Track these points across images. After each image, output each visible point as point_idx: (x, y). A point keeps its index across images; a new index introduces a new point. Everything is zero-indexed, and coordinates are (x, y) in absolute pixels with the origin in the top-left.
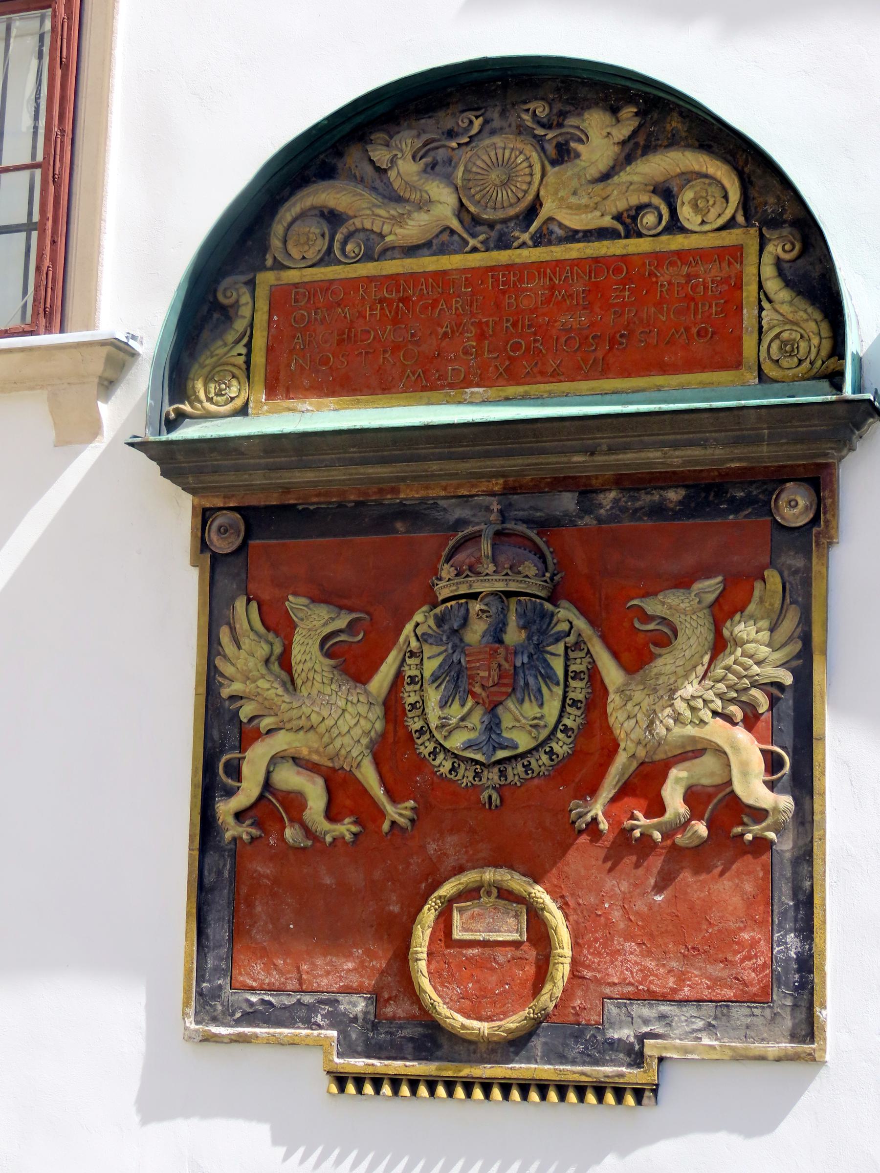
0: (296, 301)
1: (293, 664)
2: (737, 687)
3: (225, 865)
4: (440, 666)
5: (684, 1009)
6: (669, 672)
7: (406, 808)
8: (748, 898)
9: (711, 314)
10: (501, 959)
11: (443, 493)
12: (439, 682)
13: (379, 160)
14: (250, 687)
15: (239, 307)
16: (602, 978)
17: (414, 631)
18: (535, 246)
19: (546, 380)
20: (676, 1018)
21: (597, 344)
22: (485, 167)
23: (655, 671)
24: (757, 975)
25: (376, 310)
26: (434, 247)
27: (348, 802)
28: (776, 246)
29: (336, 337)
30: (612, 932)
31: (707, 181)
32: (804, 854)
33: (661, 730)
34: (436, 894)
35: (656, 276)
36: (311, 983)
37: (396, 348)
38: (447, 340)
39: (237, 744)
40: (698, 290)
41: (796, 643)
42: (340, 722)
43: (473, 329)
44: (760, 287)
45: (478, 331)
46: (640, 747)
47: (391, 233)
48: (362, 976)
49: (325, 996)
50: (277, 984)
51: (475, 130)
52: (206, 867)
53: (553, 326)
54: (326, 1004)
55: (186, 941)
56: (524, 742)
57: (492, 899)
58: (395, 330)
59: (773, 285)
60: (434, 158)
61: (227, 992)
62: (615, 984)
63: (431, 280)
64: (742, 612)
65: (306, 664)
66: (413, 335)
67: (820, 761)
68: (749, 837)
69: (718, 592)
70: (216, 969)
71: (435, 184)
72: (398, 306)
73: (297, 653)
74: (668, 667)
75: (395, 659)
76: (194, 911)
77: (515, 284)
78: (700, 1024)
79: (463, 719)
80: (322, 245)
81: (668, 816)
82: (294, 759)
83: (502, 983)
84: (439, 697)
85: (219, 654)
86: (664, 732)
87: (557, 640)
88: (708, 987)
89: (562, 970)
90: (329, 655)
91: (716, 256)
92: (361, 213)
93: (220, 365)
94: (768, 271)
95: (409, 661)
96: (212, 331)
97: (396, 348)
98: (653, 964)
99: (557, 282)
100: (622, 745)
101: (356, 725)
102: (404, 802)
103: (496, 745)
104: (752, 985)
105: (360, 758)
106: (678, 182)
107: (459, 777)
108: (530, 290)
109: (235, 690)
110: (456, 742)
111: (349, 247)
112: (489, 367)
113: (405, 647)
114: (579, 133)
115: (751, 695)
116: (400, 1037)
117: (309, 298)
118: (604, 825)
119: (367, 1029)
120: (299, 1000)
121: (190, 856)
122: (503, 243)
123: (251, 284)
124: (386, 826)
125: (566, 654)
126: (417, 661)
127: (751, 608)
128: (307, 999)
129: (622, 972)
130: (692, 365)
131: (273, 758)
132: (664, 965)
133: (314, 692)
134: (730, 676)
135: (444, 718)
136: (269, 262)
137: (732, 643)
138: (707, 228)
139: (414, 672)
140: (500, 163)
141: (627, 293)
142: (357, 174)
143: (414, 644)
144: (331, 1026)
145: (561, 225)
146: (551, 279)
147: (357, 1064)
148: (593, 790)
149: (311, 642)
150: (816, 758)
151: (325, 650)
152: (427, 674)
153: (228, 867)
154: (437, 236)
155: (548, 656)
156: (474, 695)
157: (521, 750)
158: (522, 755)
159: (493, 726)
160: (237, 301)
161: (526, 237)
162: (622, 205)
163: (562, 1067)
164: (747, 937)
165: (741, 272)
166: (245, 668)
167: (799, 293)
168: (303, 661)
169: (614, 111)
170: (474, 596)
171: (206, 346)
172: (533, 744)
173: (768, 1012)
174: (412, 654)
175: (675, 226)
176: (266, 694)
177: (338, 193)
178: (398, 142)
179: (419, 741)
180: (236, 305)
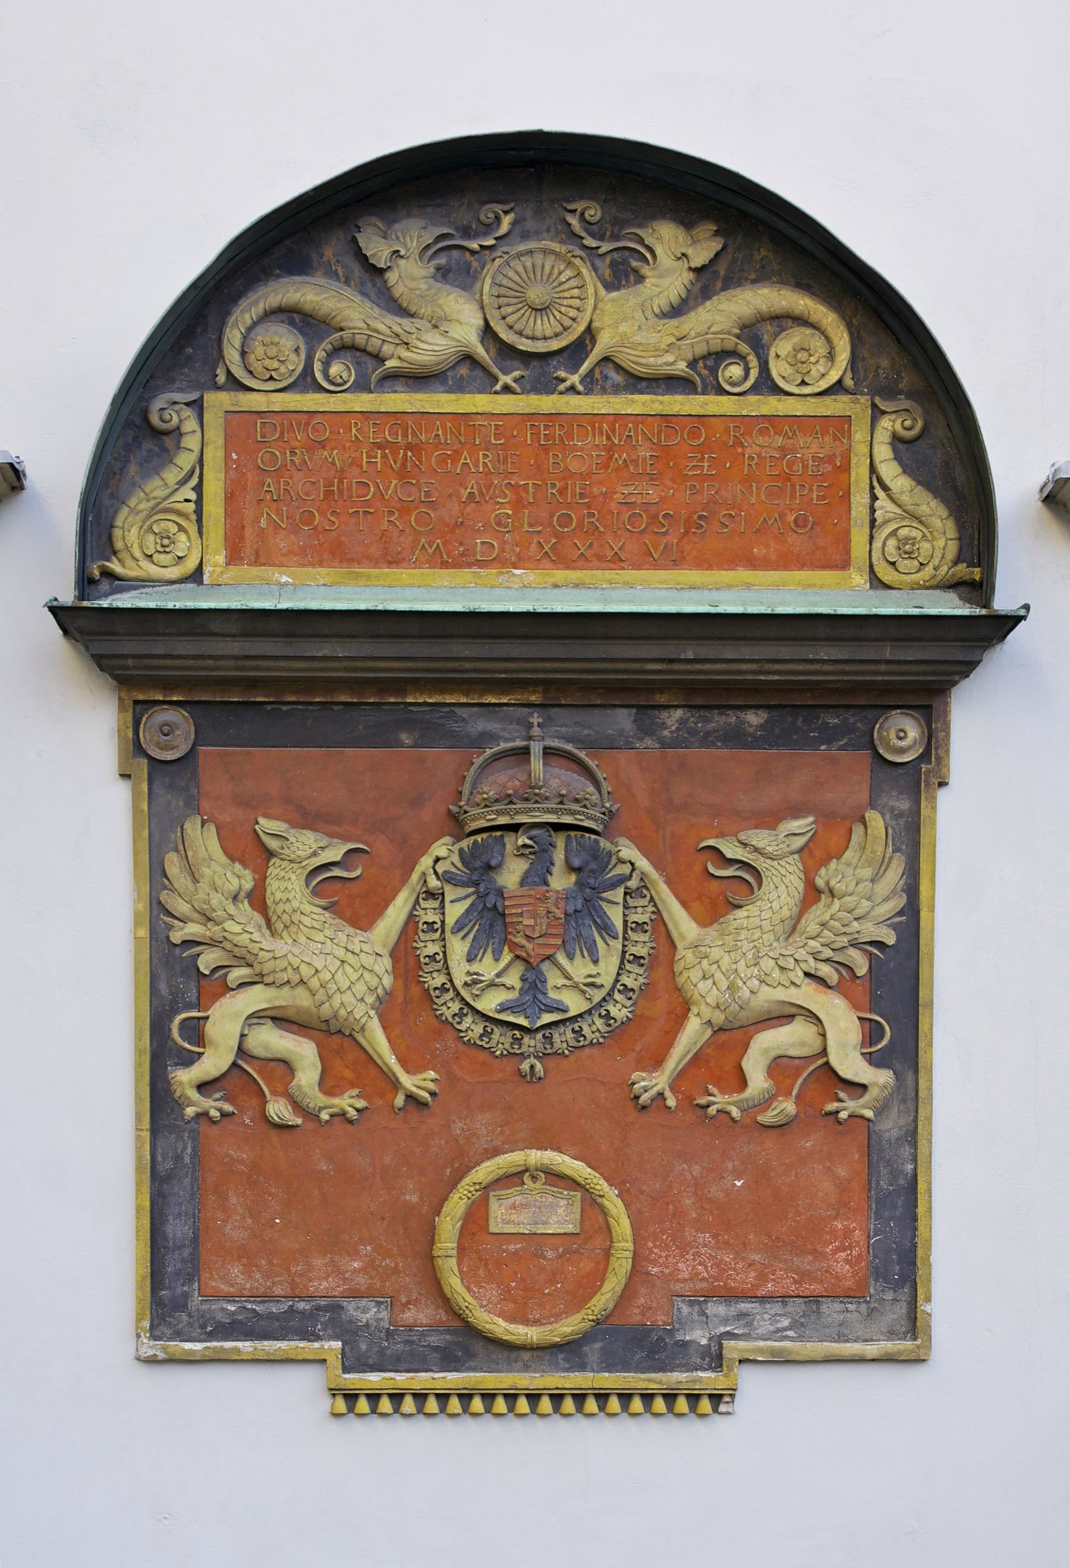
0: (263, 436)
1: (269, 902)
2: (832, 947)
3: (185, 1148)
4: (467, 911)
5: (768, 1306)
6: (753, 926)
7: (425, 1080)
8: (841, 1183)
9: (812, 499)
10: (550, 1254)
11: (464, 700)
12: (466, 930)
13: (372, 255)
14: (215, 930)
15: (181, 435)
16: (671, 1274)
17: (434, 868)
18: (586, 394)
19: (605, 565)
20: (758, 1317)
21: (670, 525)
22: (518, 279)
23: (735, 924)
24: (852, 1268)
25: (376, 457)
26: (450, 383)
27: (348, 1074)
28: (894, 421)
29: (322, 488)
30: (681, 1222)
31: (808, 331)
32: (906, 1135)
33: (745, 993)
34: (467, 1180)
35: (743, 446)
36: (306, 1288)
37: (405, 509)
38: (472, 504)
39: (194, 1000)
40: (795, 468)
41: (901, 896)
42: (339, 976)
43: (507, 492)
44: (873, 469)
45: (514, 497)
46: (717, 1012)
47: (392, 357)
48: (372, 1278)
49: (323, 1302)
50: (262, 1290)
51: (504, 228)
52: (160, 1150)
53: (612, 499)
54: (327, 1311)
55: (138, 1240)
56: (575, 1004)
57: (538, 1185)
58: (402, 486)
59: (889, 470)
60: (448, 263)
61: (196, 1300)
62: (685, 1280)
63: (449, 425)
64: (838, 859)
65: (288, 904)
66: (428, 494)
67: (926, 1030)
68: (843, 1115)
69: (810, 835)
70: (178, 1273)
71: (452, 296)
72: (405, 455)
73: (275, 888)
74: (751, 920)
75: (406, 901)
76: (147, 1204)
77: (562, 440)
78: (786, 1322)
79: (498, 975)
80: (296, 364)
81: (749, 1093)
82: (274, 1019)
83: (552, 1281)
84: (466, 949)
85: (165, 888)
86: (747, 993)
87: (613, 885)
88: (795, 1282)
89: (621, 1265)
90: (315, 893)
91: (817, 427)
92: (351, 325)
93: (154, 514)
94: (883, 452)
95: (424, 904)
96: (141, 464)
97: (405, 509)
98: (731, 1257)
99: (616, 442)
100: (695, 1010)
101: (358, 979)
102: (421, 1073)
103: (543, 1008)
104: (845, 1278)
105: (364, 1020)
106: (769, 328)
107: (493, 1043)
108: (581, 449)
109: (191, 934)
110: (489, 1003)
111: (335, 369)
112: (530, 544)
113: (419, 887)
114: (643, 250)
115: (848, 956)
116: (422, 1346)
117: (282, 433)
118: (671, 1102)
119: (381, 1338)
120: (291, 1307)
121: (138, 1138)
122: (546, 385)
123: (197, 406)
124: (400, 1100)
125: (625, 900)
126: (436, 904)
127: (848, 854)
128: (302, 1305)
129: (694, 1267)
130: (786, 561)
131: (249, 1017)
132: (743, 1258)
133: (302, 939)
134: (826, 932)
135: (475, 974)
136: (221, 379)
137: (829, 894)
138: (807, 390)
139: (431, 917)
140: (539, 278)
141: (706, 464)
142: (340, 271)
143: (433, 883)
144: (335, 1337)
145: (619, 368)
146: (609, 438)
147: (371, 1378)
148: (657, 1062)
149: (293, 877)
150: (923, 1027)
151: (311, 888)
152: (450, 921)
153: (189, 1150)
154: (453, 367)
155: (604, 905)
156: (514, 946)
157: (572, 1013)
158: (574, 1019)
159: (534, 984)
160: (178, 428)
161: (575, 379)
162: (701, 350)
163: (627, 1374)
164: (840, 1226)
165: (849, 450)
166: (205, 907)
167: (919, 483)
168: (284, 901)
169: (688, 224)
170: (514, 828)
171: (134, 484)
172: (585, 1006)
173: (864, 1307)
174: (430, 895)
175: (767, 385)
176: (237, 940)
177: (317, 295)
178: (399, 234)
179: (440, 1001)
180: (177, 433)
